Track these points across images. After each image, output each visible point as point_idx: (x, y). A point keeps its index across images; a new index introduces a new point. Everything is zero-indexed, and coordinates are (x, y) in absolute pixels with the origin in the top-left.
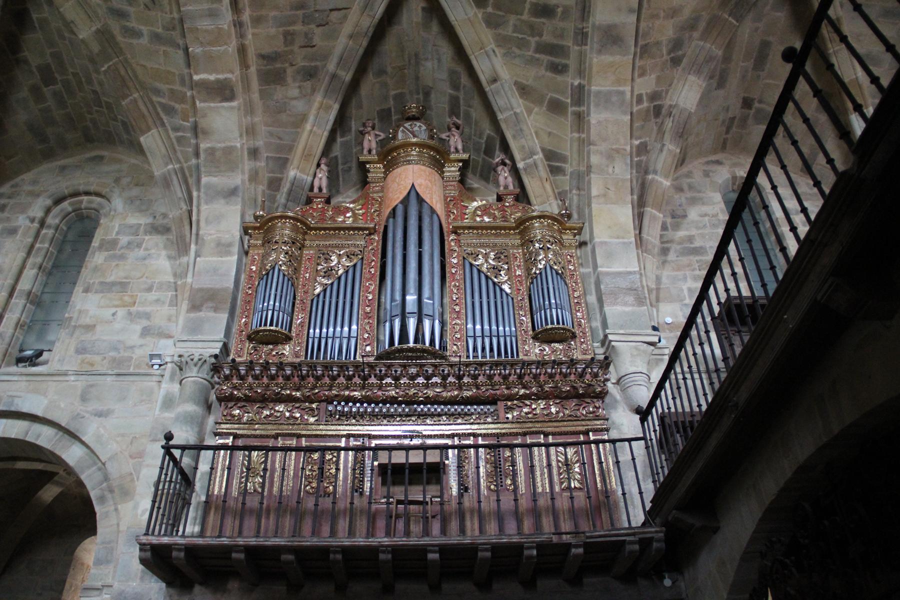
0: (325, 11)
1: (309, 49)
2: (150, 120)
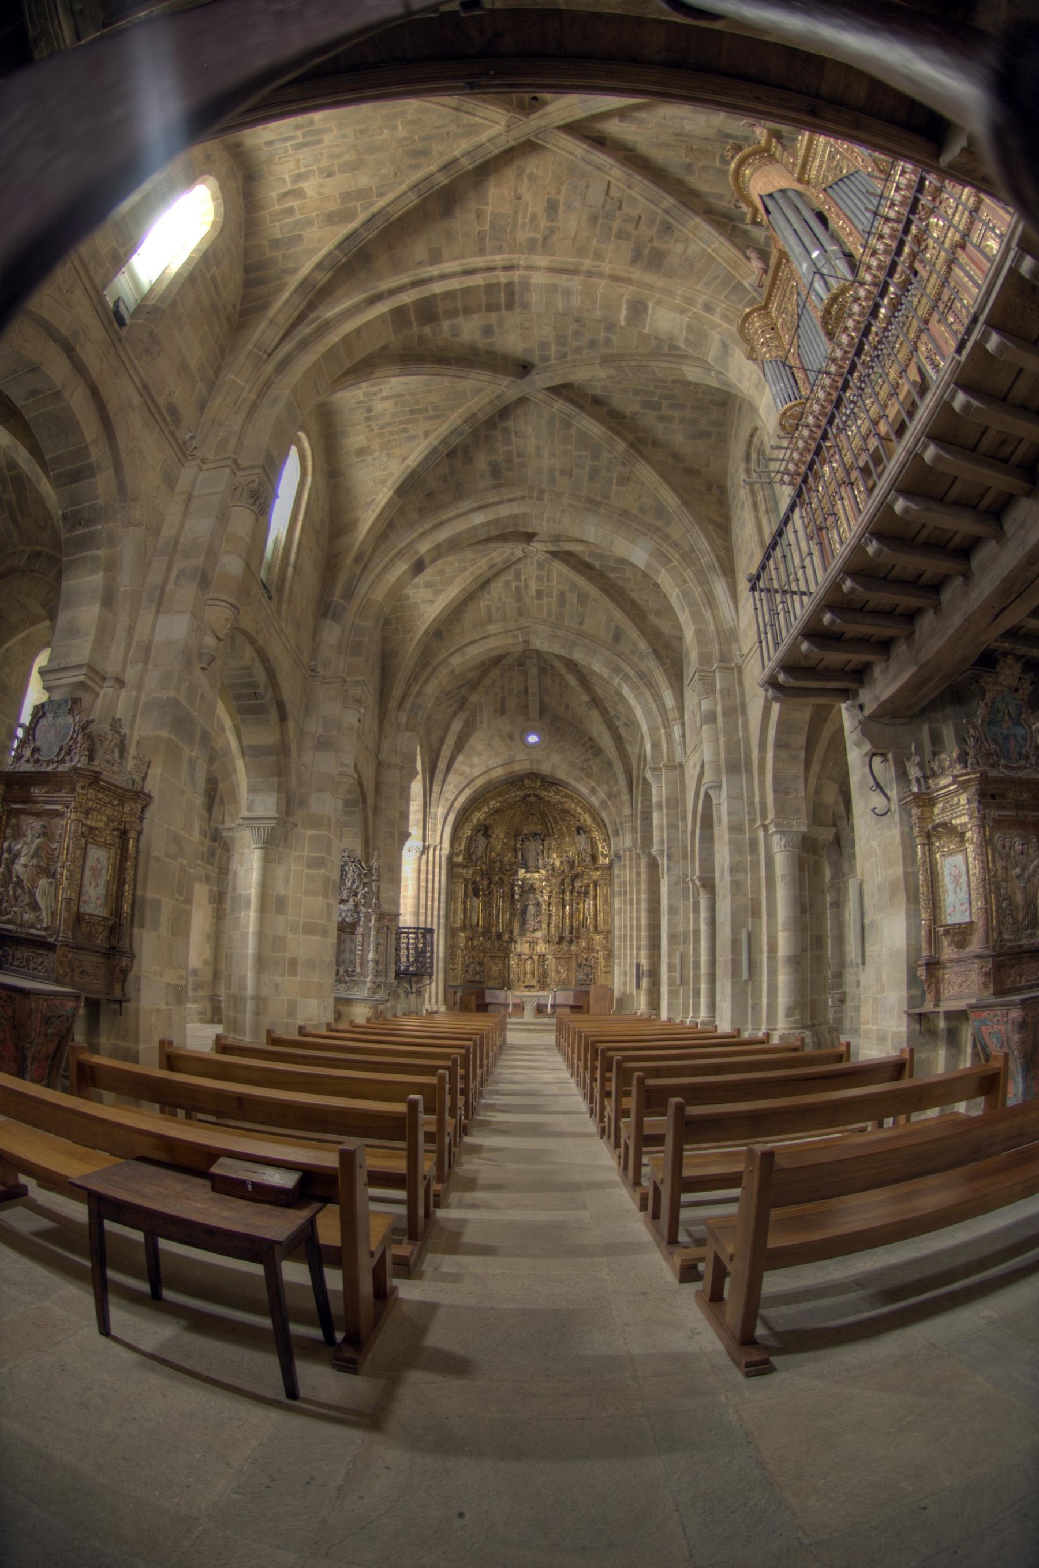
0: (605, 201)
1: (642, 222)
2: (674, 366)
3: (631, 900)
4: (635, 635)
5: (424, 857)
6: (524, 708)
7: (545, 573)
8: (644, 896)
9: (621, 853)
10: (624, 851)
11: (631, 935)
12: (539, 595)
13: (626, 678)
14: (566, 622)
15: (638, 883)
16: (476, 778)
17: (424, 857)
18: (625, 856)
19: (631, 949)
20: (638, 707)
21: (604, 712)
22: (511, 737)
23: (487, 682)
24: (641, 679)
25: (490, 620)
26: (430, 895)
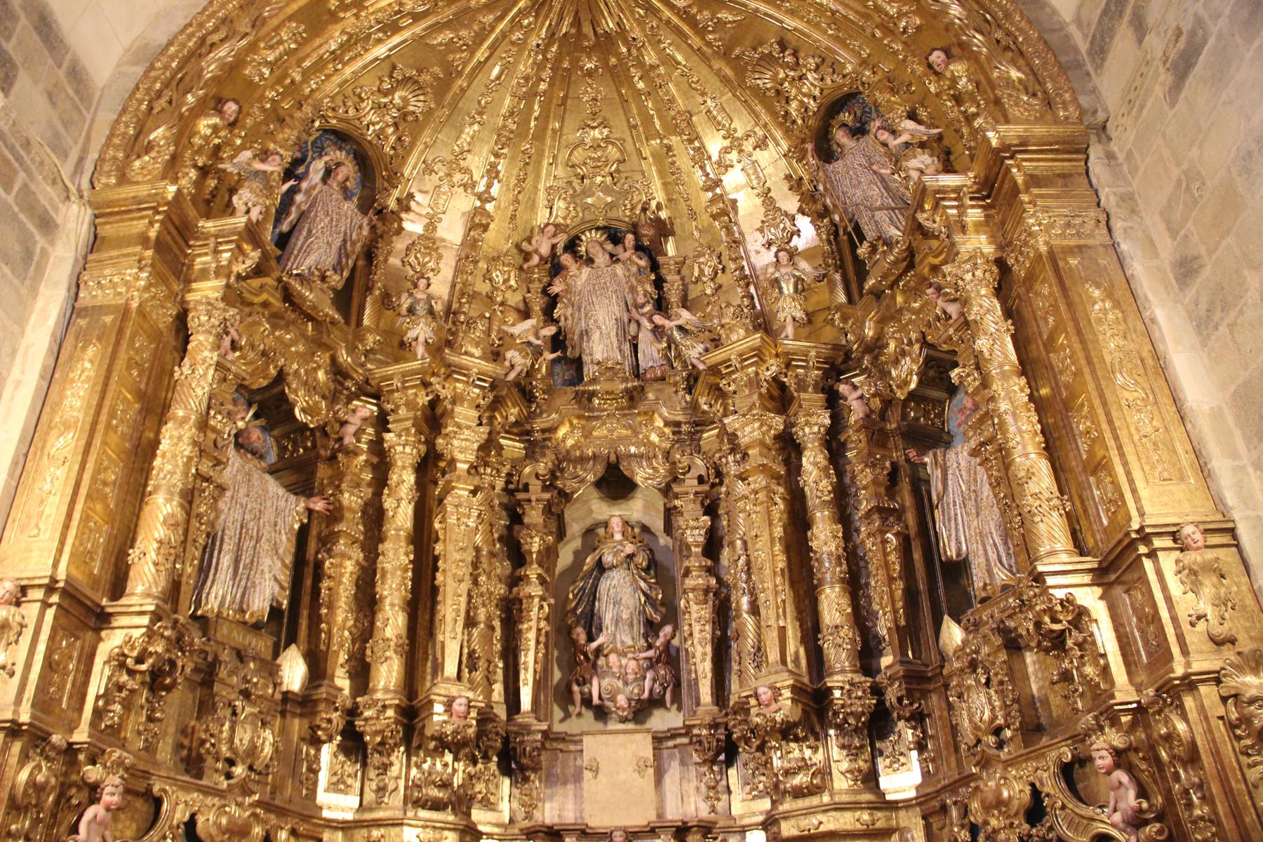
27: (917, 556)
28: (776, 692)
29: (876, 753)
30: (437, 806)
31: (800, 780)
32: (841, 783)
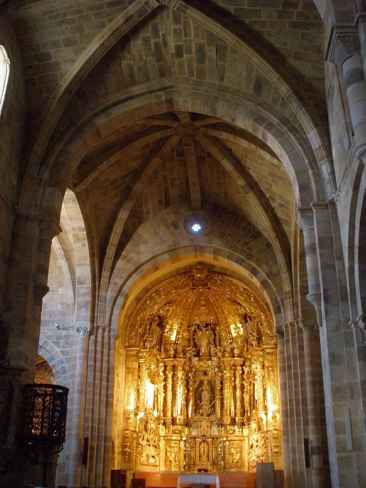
3: (296, 374)
4: (275, 79)
5: (93, 337)
6: (186, 198)
7: (182, 27)
8: (307, 369)
9: (284, 328)
10: (286, 326)
11: (298, 410)
12: (179, 52)
13: (270, 127)
14: (207, 80)
15: (302, 356)
16: (143, 264)
17: (93, 337)
18: (287, 331)
19: (299, 424)
20: (284, 153)
21: (261, 195)
22: (175, 226)
23: (149, 171)
24: (285, 125)
25: (134, 83)
26: (98, 374)
27: (252, 398)
28: (228, 420)
29: (243, 428)
30: (177, 433)
31: (231, 432)
32: (237, 433)
